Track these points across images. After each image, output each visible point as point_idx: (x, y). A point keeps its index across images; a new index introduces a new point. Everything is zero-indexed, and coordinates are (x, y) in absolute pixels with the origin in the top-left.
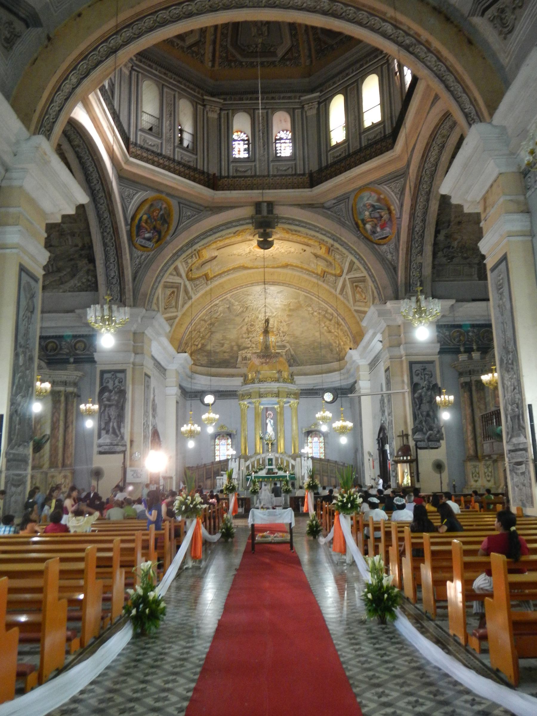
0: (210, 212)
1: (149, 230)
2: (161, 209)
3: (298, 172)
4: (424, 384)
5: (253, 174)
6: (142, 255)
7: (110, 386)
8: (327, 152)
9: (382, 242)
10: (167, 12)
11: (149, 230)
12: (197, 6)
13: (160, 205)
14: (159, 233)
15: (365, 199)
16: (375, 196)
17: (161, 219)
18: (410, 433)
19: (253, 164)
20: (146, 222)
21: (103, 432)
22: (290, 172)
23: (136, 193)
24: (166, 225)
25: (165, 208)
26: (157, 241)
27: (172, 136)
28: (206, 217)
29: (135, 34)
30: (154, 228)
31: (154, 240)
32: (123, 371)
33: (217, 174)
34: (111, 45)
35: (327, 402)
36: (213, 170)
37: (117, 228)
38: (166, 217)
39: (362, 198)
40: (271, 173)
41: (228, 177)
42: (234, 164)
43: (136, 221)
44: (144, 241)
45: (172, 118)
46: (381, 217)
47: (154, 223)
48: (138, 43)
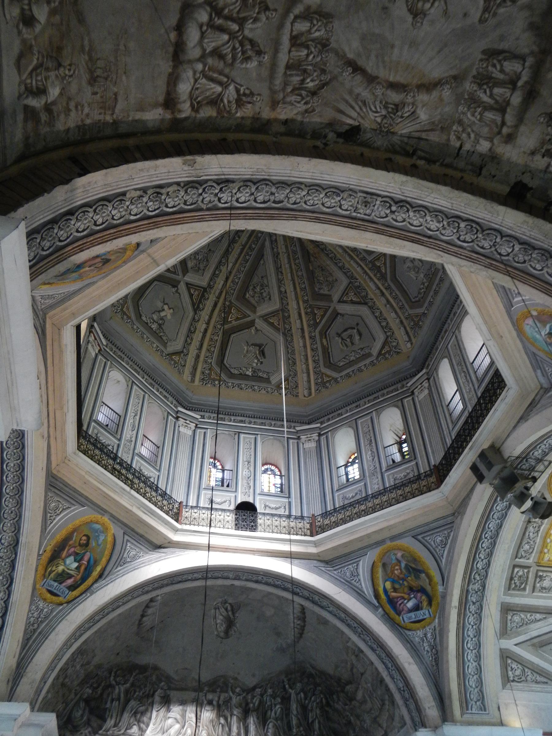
0: (459, 517)
1: (406, 596)
2: (399, 561)
6: (425, 635)
10: (7, 484)
11: (406, 596)
12: (12, 459)
13: (394, 558)
14: (422, 590)
15: (538, 336)
17: (410, 572)
20: (395, 590)
23: (357, 566)
24: (424, 575)
25: (403, 556)
26: (430, 604)
27: (377, 465)
29: (14, 519)
30: (411, 589)
31: (425, 604)
34: (6, 544)
37: (361, 623)
38: (413, 566)
43: (383, 596)
44: (412, 615)
45: (374, 444)
47: (405, 583)
48: (26, 519)
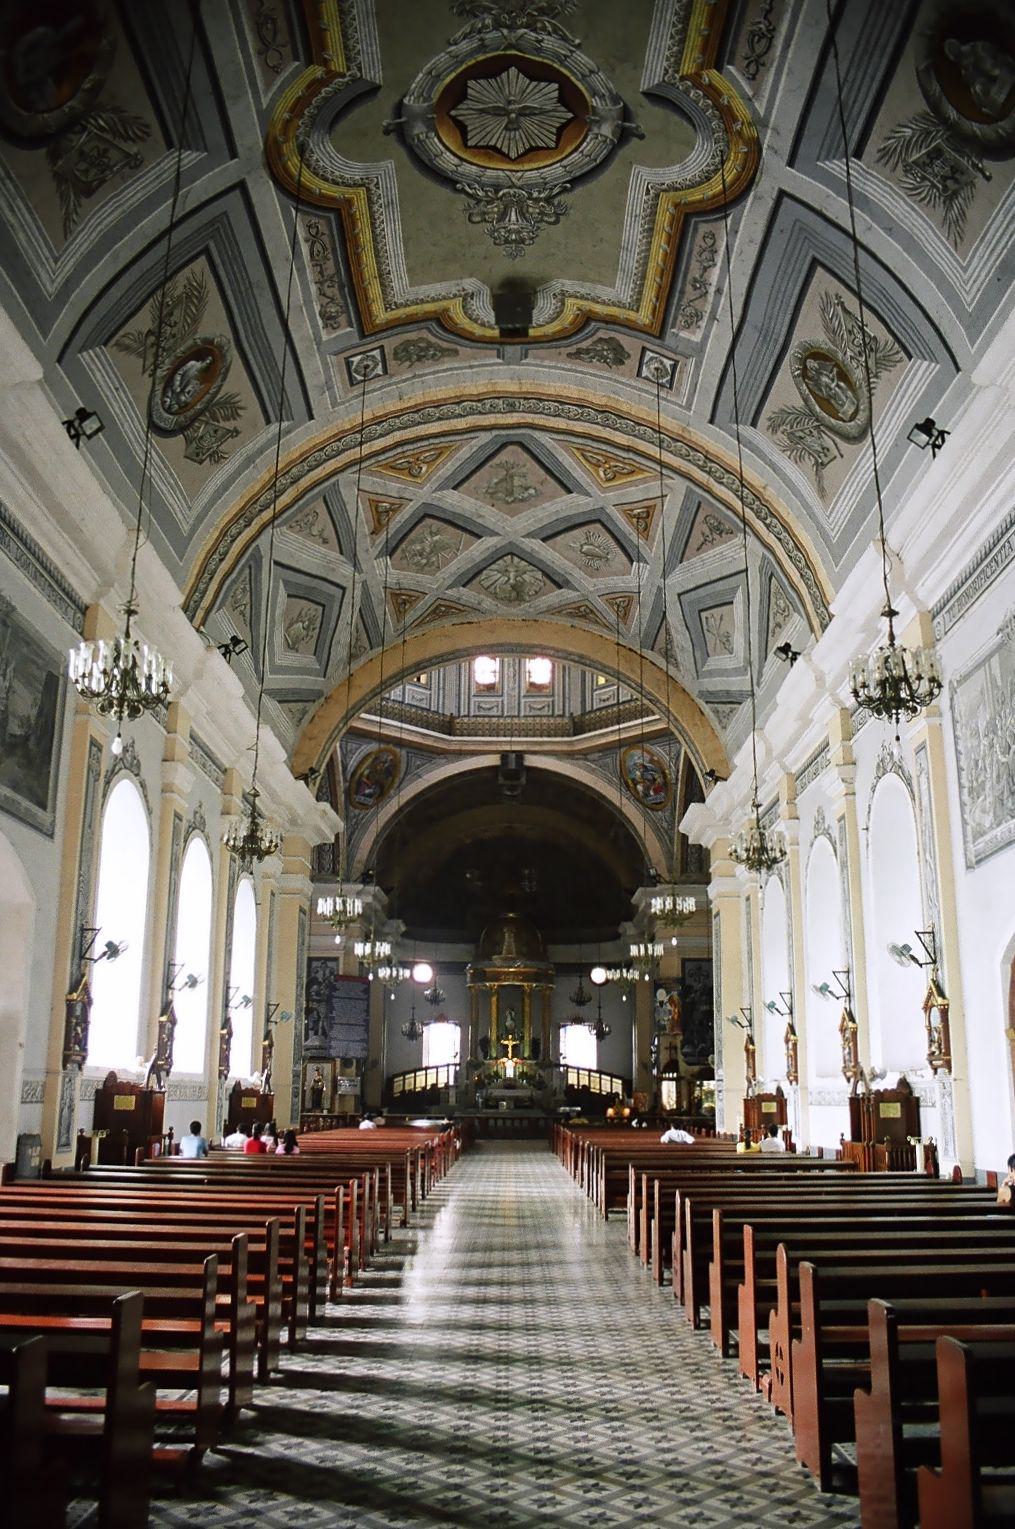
3: (556, 713)
4: (698, 986)
5: (499, 713)
7: (320, 976)
8: (593, 691)
9: (658, 807)
16: (647, 757)
18: (679, 1046)
19: (500, 699)
20: (368, 778)
21: (311, 1033)
22: (545, 712)
28: (440, 766)
32: (336, 959)
33: (455, 714)
35: (595, 984)
36: (450, 709)
39: (632, 756)
40: (522, 714)
41: (468, 716)
42: (477, 699)
43: (357, 776)
46: (655, 780)
